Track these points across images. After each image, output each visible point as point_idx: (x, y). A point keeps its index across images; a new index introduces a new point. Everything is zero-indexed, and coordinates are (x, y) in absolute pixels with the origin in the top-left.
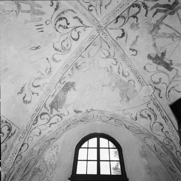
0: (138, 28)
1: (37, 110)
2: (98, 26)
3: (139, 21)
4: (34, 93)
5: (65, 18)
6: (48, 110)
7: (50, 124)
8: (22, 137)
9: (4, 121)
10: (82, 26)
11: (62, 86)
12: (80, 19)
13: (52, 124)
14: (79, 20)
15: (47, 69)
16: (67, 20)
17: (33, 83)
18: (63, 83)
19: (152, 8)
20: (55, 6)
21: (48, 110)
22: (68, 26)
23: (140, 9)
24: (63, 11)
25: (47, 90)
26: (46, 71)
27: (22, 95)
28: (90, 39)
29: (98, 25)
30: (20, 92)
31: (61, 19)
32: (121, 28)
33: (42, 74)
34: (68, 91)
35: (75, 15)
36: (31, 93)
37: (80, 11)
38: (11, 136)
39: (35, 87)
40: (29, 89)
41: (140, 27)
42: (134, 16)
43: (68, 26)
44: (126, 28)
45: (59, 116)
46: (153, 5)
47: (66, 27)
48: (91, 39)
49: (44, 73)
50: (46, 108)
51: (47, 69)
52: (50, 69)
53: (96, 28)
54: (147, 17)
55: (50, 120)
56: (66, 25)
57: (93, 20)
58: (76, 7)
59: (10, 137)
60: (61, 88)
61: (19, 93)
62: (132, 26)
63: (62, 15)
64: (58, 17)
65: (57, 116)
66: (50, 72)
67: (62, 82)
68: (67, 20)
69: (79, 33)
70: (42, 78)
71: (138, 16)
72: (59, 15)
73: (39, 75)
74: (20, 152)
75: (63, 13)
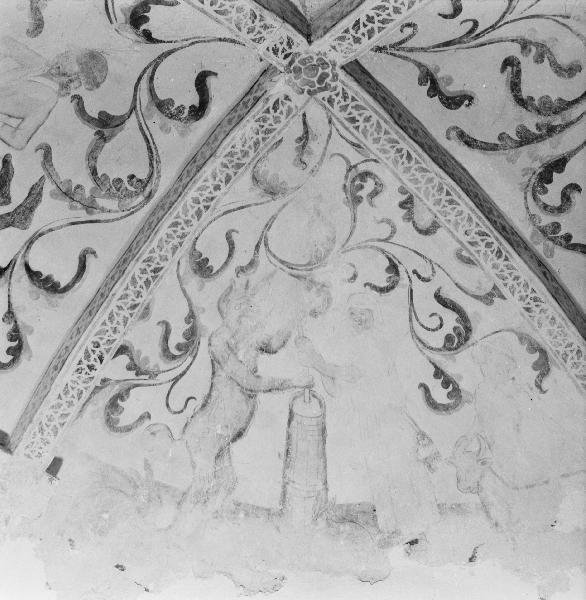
0: (57, 72)
2: (325, 89)
3: (66, 106)
5: (522, 102)
10: (423, 49)
12: (435, 90)
14: (442, 85)
16: (515, 86)
19: (35, 195)
20: (560, 181)
22: (514, 50)
23: (94, 172)
24: (525, 149)
28: (383, 22)
29: (326, 94)
31: (547, 107)
32: (170, 47)
35: (461, 117)
37: (433, 175)
41: (41, 80)
42: (106, 125)
43: (514, 50)
44: (127, 55)
46: (39, 210)
47: (534, 49)
48: (370, 19)
53: (335, 77)
54: (36, 141)
56: (527, 63)
57: (353, 120)
58: (448, 194)
62: (94, 65)
63: (534, 130)
64: (557, 121)
68: (515, 86)
69: (449, 10)
71: (89, 133)
72: (551, 130)
75: (526, 139)
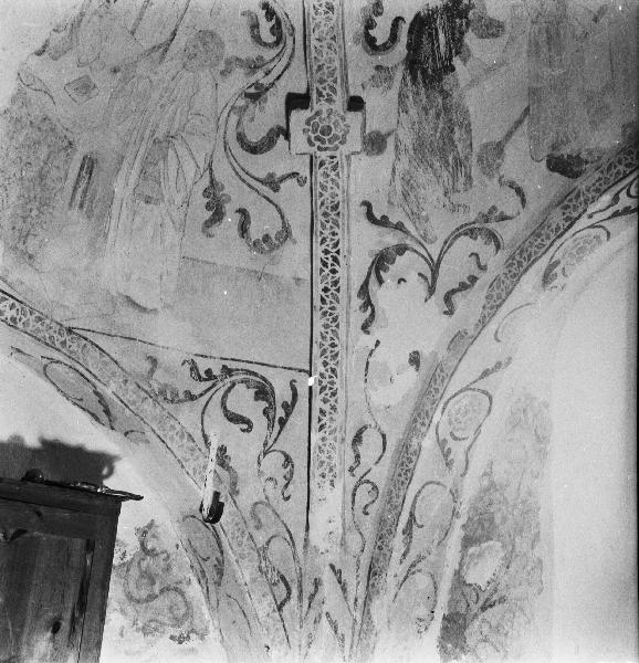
1: (330, 261)
4: (279, 174)
6: (399, 227)
7: (448, 298)
8: (326, 407)
9: (216, 372)
11: (401, 49)
13: (453, 291)
15: (255, 26)
17: (241, 138)
18: (394, 37)
21: (399, 227)
25: (318, 143)
26: (257, 39)
27: (231, 219)
30: (208, 215)
33: (253, 66)
34: (457, 61)
36: (266, 190)
38: (288, 415)
39: (254, 150)
40: (242, 175)
45: (471, 233)
49: (250, 51)
50: (383, 222)
51: (255, 26)
52: (270, 13)
55: (435, 269)
59: (283, 422)
60: (398, 75)
61: (209, 224)
65: (464, 240)
66: (277, 29)
67: (381, 33)
70: (266, 81)
73: (239, 81)
74: (359, 472)
